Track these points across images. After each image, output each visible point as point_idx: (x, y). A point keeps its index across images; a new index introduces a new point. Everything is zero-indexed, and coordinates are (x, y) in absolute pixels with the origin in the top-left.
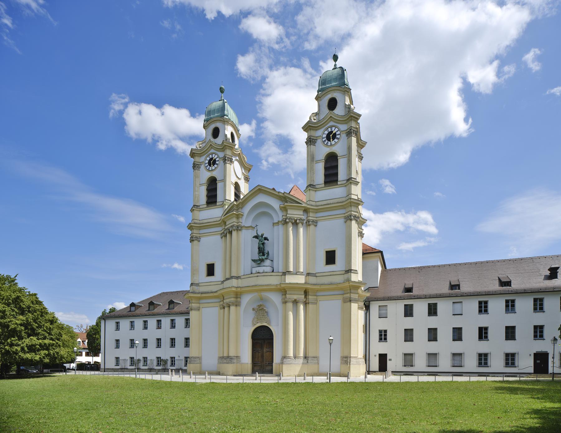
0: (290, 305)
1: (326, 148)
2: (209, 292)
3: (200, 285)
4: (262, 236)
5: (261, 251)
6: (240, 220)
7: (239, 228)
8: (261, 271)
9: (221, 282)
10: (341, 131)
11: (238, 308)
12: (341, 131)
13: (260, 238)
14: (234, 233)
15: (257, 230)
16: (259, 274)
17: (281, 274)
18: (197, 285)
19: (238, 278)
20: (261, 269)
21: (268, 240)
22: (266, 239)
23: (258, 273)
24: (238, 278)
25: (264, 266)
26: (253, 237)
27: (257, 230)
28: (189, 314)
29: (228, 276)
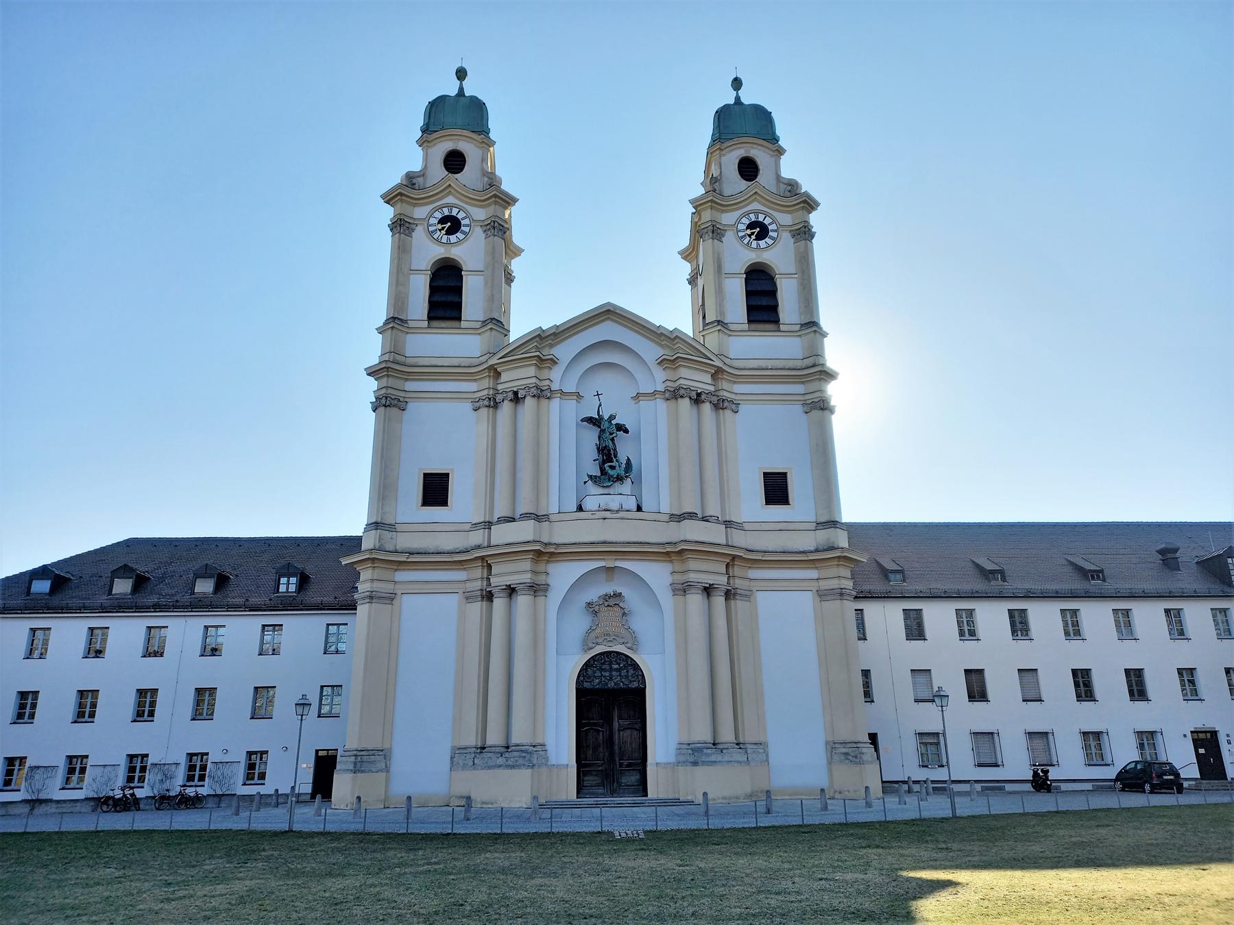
0: (695, 600)
1: (747, 252)
2: (431, 551)
3: (399, 527)
4: (612, 417)
5: (606, 454)
6: (545, 374)
7: (542, 394)
8: (615, 506)
9: (470, 525)
10: (779, 226)
11: (541, 599)
12: (779, 226)
13: (606, 425)
14: (529, 402)
15: (600, 405)
16: (608, 514)
17: (666, 518)
18: (391, 527)
19: (538, 518)
20: (613, 502)
21: (626, 431)
22: (621, 428)
23: (605, 510)
24: (538, 518)
25: (621, 494)
26: (583, 420)
27: (600, 405)
28: (356, 609)
29: (501, 510)
